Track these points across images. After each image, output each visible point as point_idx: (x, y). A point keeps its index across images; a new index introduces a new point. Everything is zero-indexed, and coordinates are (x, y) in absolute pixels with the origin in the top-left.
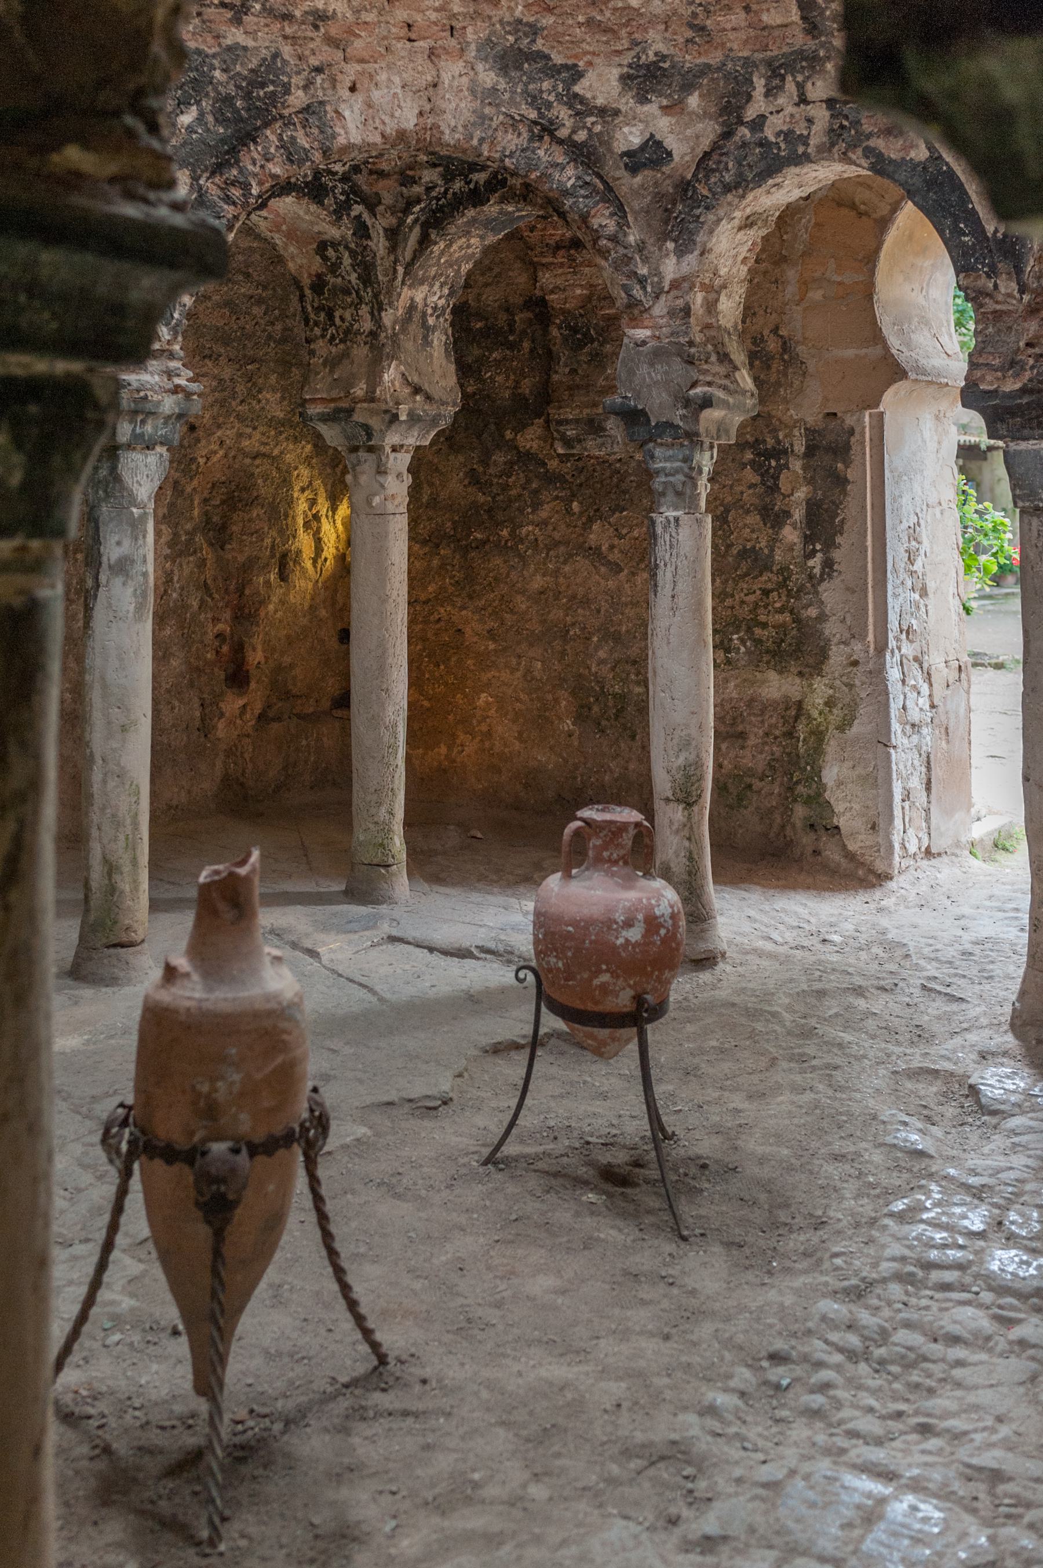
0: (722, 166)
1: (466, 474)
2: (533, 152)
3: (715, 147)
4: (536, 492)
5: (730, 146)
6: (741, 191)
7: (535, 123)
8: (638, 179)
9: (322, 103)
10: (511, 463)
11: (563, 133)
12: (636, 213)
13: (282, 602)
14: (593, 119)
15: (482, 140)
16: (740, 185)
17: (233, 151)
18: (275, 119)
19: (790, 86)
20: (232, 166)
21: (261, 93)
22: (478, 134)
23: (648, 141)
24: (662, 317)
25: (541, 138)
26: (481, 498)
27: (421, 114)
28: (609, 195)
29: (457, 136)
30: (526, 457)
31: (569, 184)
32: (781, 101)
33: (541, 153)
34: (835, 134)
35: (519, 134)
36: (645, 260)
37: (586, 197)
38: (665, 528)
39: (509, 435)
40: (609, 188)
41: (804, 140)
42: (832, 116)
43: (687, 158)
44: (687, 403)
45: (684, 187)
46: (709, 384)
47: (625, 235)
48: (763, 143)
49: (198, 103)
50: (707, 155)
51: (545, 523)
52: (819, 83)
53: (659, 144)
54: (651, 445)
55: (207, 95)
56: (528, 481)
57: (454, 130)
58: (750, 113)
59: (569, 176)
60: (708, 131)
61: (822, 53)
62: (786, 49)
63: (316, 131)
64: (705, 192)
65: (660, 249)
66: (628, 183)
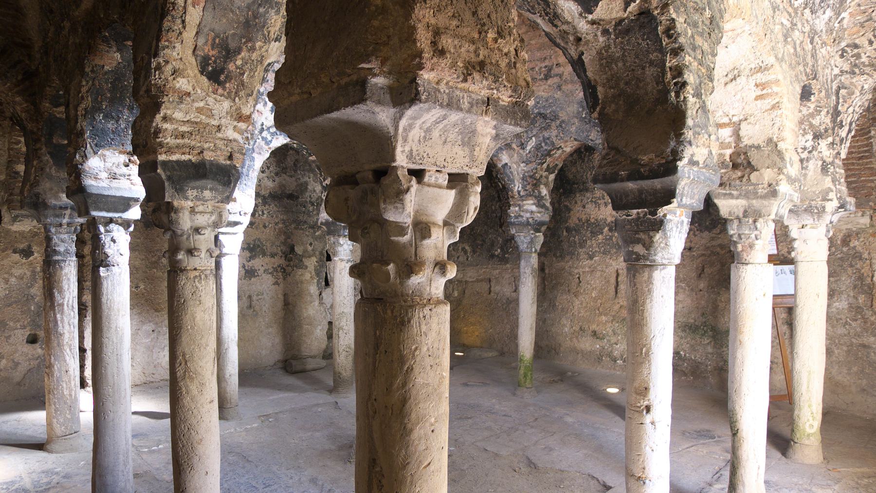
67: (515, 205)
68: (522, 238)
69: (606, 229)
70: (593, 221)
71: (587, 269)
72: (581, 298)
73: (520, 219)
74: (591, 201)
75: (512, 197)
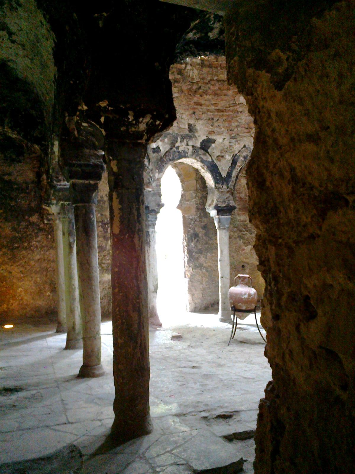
1: (12, 228)
4: (36, 233)
10: (28, 225)
12: (152, 162)
19: (185, 141)
26: (17, 235)
30: (32, 224)
32: (183, 144)
34: (193, 153)
36: (152, 173)
39: (26, 217)
41: (187, 153)
42: (193, 149)
48: (179, 152)
50: (167, 152)
52: (191, 142)
53: (159, 148)
54: (149, 215)
58: (177, 145)
60: (168, 147)
61: (192, 136)
62: (184, 133)
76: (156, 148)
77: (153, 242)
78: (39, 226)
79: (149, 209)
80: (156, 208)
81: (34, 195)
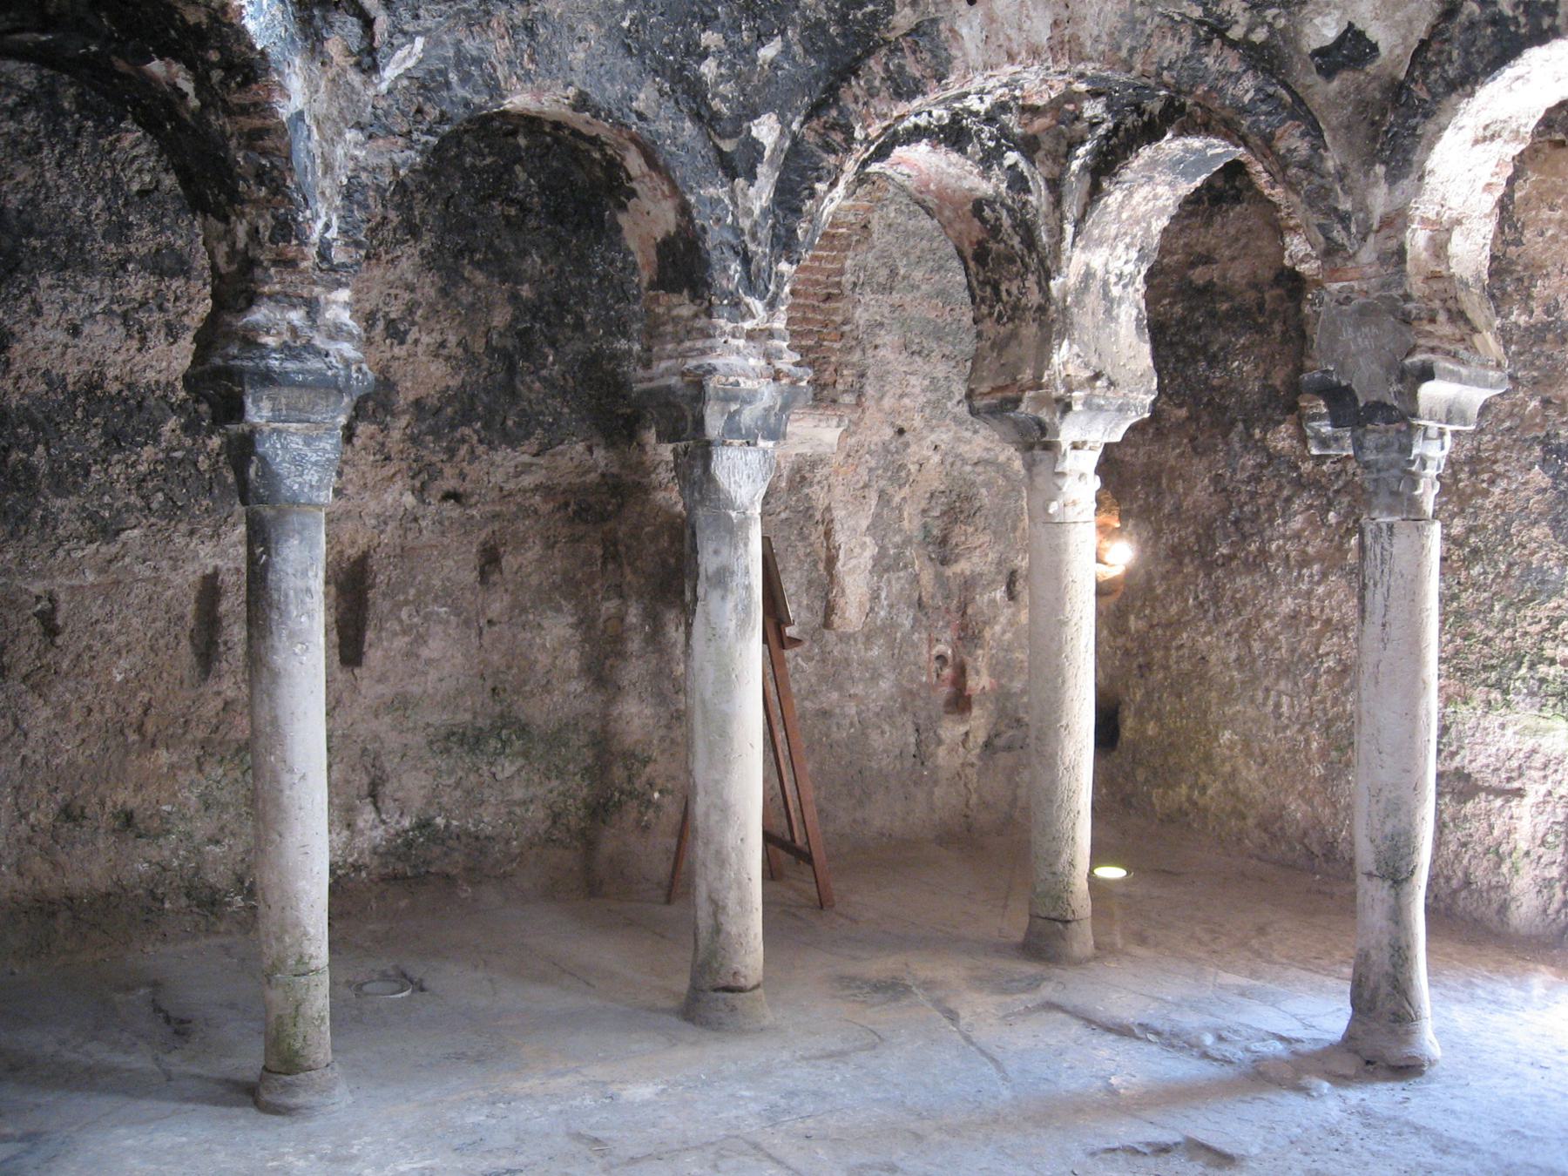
0: (1444, 57)
2: (1199, 61)
3: (1435, 32)
5: (1455, 29)
6: (1468, 88)
7: (1200, 23)
8: (1335, 84)
9: (934, 21)
11: (1236, 33)
13: (1011, 623)
14: (1275, 11)
15: (1132, 51)
16: (1468, 80)
17: (832, 90)
18: (878, 46)
20: (830, 107)
21: (859, 15)
22: (1127, 43)
23: (1346, 32)
24: (1370, 265)
25: (1208, 42)
27: (1056, 24)
28: (1300, 111)
29: (1101, 47)
31: (1246, 99)
33: (1209, 61)
35: (1181, 40)
36: (1348, 192)
37: (1269, 114)
38: (1376, 538)
40: (1299, 101)
43: (1398, 51)
44: (1403, 375)
45: (1397, 92)
46: (1433, 350)
47: (1322, 159)
49: (783, 33)
50: (1424, 45)
51: (1297, 535)
55: (793, 23)
56: (1280, 488)
57: (1097, 40)
59: (1246, 88)
63: (927, 56)
64: (1424, 95)
65: (1366, 175)
66: (1322, 91)
67: (287, 299)
68: (296, 443)
69: (173, 423)
70: (113, 388)
71: (91, 577)
72: (61, 691)
73: (315, 364)
74: (108, 312)
75: (290, 264)
76: (1341, 41)
77: (1381, 590)
78: (1297, 468)
79: (1355, 400)
80: (1390, 393)
81: (1284, 333)
